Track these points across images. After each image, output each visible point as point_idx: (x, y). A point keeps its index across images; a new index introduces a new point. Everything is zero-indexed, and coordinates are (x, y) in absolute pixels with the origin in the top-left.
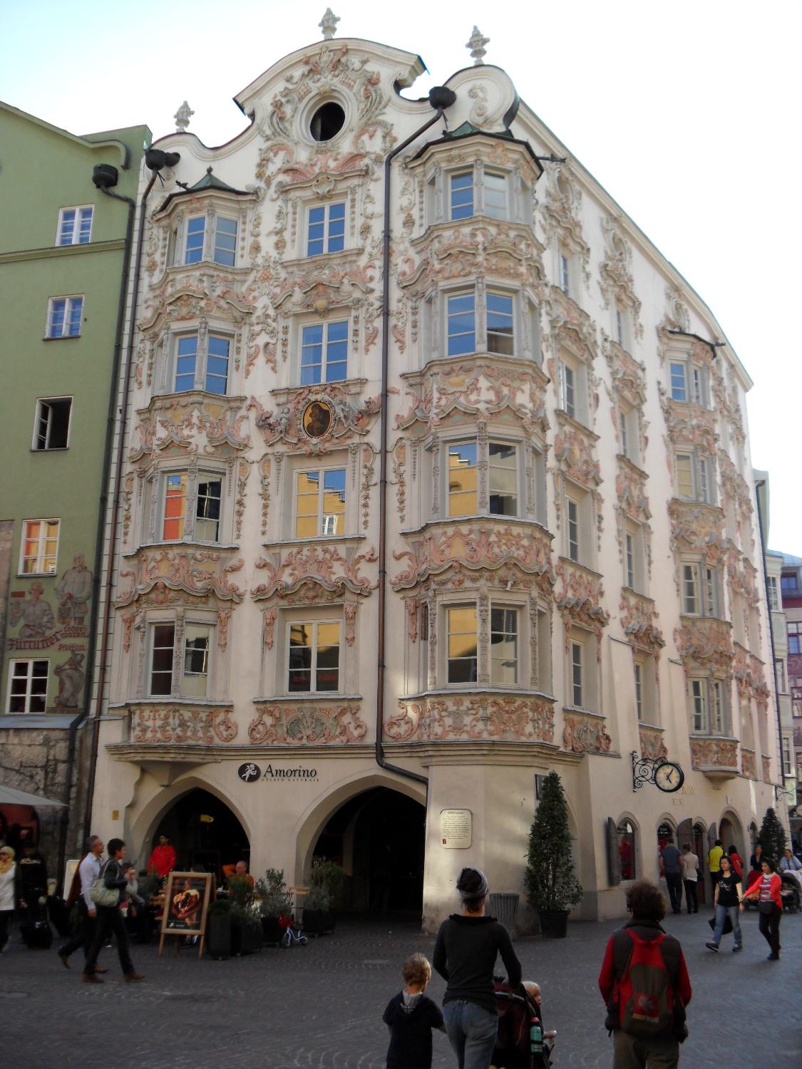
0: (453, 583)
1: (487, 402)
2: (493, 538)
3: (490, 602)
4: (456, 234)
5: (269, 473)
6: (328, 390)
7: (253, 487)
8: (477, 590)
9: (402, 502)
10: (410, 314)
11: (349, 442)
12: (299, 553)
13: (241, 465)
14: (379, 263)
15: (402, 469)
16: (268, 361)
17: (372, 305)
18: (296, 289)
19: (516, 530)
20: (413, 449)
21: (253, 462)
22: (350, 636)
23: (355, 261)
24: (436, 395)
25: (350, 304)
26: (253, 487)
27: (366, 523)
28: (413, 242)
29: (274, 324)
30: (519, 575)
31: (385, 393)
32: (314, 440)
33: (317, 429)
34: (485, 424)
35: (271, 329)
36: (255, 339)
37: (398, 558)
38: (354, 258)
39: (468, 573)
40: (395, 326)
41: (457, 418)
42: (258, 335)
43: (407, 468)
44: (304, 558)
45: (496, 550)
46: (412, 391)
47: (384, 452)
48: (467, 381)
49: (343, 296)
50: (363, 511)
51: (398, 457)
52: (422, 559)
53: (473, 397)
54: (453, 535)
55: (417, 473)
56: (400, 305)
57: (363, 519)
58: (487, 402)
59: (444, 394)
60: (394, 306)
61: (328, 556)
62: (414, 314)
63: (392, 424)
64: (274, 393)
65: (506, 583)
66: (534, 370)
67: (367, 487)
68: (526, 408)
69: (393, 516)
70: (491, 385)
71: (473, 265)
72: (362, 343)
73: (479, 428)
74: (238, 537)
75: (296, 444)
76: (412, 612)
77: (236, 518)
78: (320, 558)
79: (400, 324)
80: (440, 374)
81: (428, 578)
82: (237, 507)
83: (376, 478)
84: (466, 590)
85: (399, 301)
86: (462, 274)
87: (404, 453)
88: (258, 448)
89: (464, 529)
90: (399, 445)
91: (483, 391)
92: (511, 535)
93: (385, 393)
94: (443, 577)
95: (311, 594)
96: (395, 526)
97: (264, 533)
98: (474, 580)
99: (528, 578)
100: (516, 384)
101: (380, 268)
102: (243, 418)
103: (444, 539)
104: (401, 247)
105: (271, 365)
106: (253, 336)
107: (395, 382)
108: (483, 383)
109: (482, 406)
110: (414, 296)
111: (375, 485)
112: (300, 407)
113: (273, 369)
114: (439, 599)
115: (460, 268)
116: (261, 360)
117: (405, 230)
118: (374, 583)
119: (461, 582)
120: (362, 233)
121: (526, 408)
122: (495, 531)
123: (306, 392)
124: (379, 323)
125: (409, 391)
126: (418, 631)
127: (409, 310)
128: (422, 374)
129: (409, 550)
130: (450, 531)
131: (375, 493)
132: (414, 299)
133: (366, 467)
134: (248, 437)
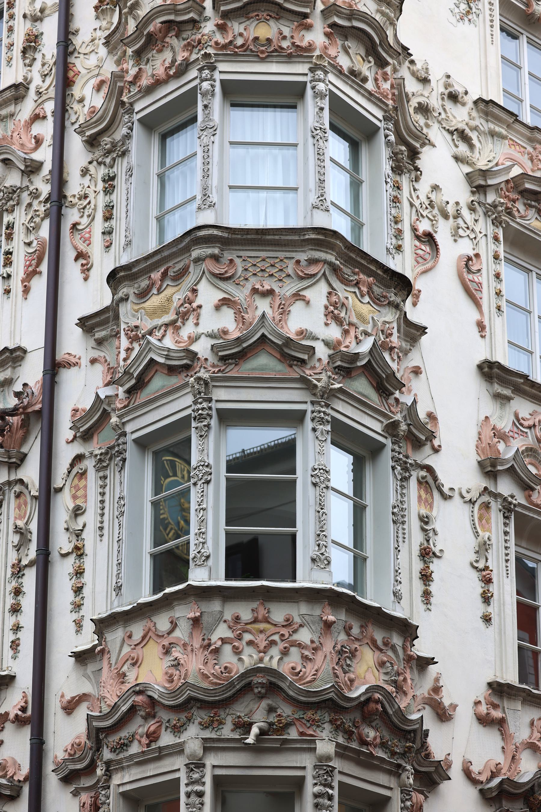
1: (211, 336)
2: (222, 631)
8: (178, 750)
9: (78, 590)
19: (279, 613)
20: (101, 474)
23: (12, 115)
30: (286, 711)
31: (54, 367)
34: (206, 384)
38: (11, 109)
39: (164, 715)
41: (159, 383)
45: (227, 656)
46: (102, 354)
47: (47, 493)
48: (176, 297)
51: (74, 497)
53: (188, 330)
54: (143, 638)
55: (106, 525)
56: (86, 181)
58: (211, 336)
60: (75, 185)
62: (109, 190)
63: (64, 430)
65: (246, 727)
66: (340, 255)
68: (316, 339)
70: (222, 295)
80: (132, 298)
84: (162, 754)
87: (85, 487)
90: (75, 471)
91: (207, 312)
92: (266, 620)
98: (177, 730)
99: (309, 714)
100: (289, 288)
104: (94, 63)
107: (73, 342)
108: (208, 295)
109: (202, 348)
110: (109, 152)
114: (116, 780)
117: (97, 24)
119: (153, 737)
120: (24, 52)
121: (316, 339)
122: (228, 616)
125: (96, 354)
127: (101, 185)
130: (138, 630)
132: (108, 160)
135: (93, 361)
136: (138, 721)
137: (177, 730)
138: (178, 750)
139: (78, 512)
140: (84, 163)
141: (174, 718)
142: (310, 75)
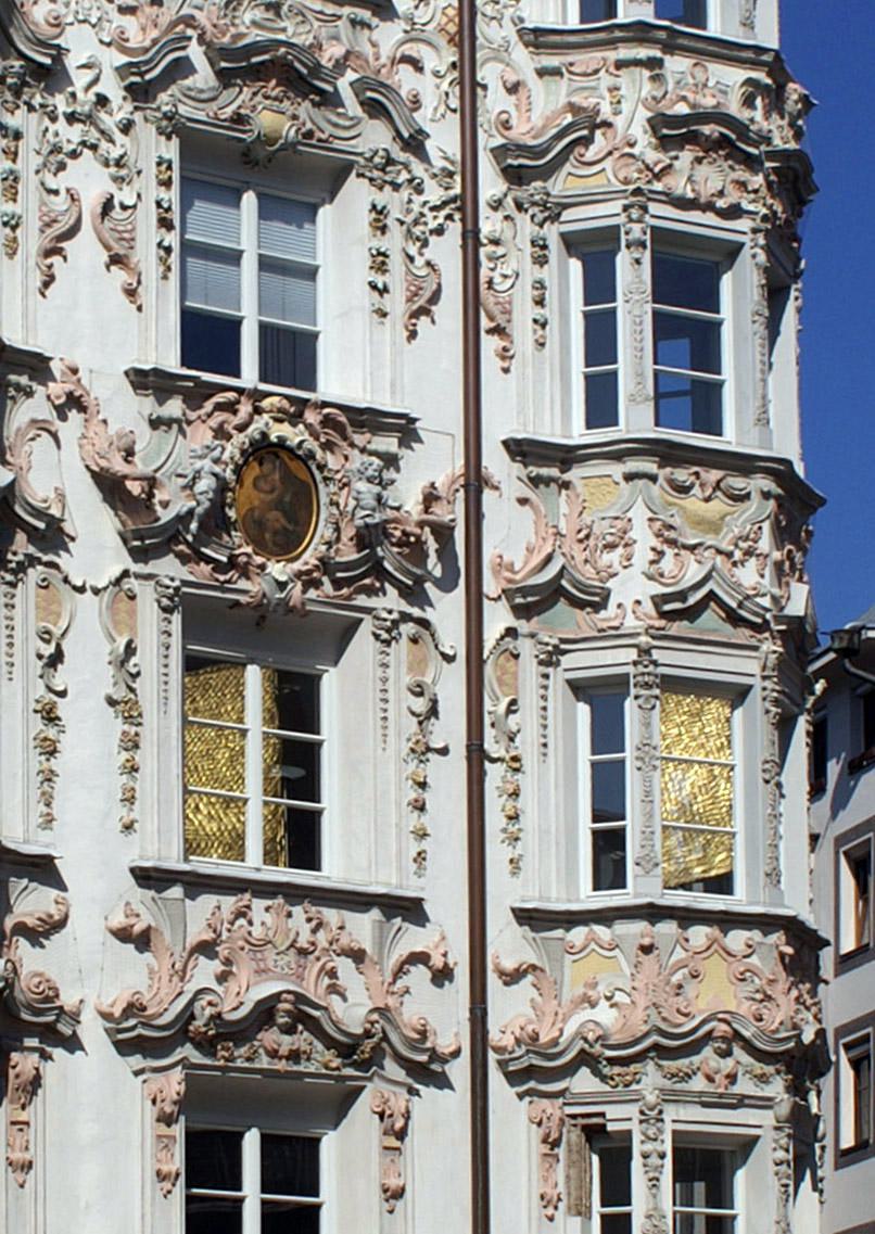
0: (710, 1079)
3: (669, 1127)
4: (698, 72)
5: (133, 629)
6: (312, 417)
7: (88, 674)
10: (529, 260)
11: (362, 600)
12: (240, 914)
13: (45, 585)
14: (438, 58)
15: (513, 722)
16: (116, 260)
17: (419, 190)
18: (195, 52)
20: (544, 670)
21: (81, 590)
22: (394, 1183)
24: (644, 538)
25: (361, 160)
26: (88, 674)
27: (421, 857)
28: (538, 39)
29: (118, 136)
31: (475, 482)
32: (278, 570)
33: (275, 533)
35: (115, 153)
36: (62, 167)
37: (512, 978)
39: (746, 1059)
40: (490, 283)
42: (74, 155)
43: (526, 721)
44: (257, 931)
49: (336, 125)
50: (413, 820)
52: (570, 991)
54: (708, 948)
57: (414, 848)
59: (672, 543)
61: (322, 938)
64: (146, 381)
67: (422, 752)
69: (497, 854)
71: (742, 185)
72: (397, 303)
73: (764, 668)
74: (49, 821)
75: (218, 567)
76: (554, 1136)
77: (37, 761)
78: (303, 942)
79: (497, 279)
81: (647, 1050)
82: (37, 723)
83: (451, 728)
84: (741, 1102)
85: (497, 205)
86: (721, 203)
87: (515, 675)
88: (97, 544)
89: (737, 939)
93: (475, 482)
94: (683, 1063)
95: (286, 1043)
96: (503, 894)
97: (128, 827)
98: (763, 1079)
101: (436, 74)
102: (41, 426)
103: (679, 954)
105: (119, 276)
106: (58, 158)
111: (444, 751)
112: (231, 450)
113: (131, 293)
115: (715, 184)
116: (86, 250)
118: (451, 1032)
119: (732, 1078)
123: (245, 408)
124: (447, 252)
126: (561, 1188)
128: (567, 456)
129: (531, 958)
131: (449, 776)
133: (418, 691)
134: (61, 497)
135: (523, 501)
136: (708, 1051)
137: (763, 1079)
138: (766, 1103)
139: (512, 707)
140: (499, 195)
141: (759, 1068)
142: (751, 236)
